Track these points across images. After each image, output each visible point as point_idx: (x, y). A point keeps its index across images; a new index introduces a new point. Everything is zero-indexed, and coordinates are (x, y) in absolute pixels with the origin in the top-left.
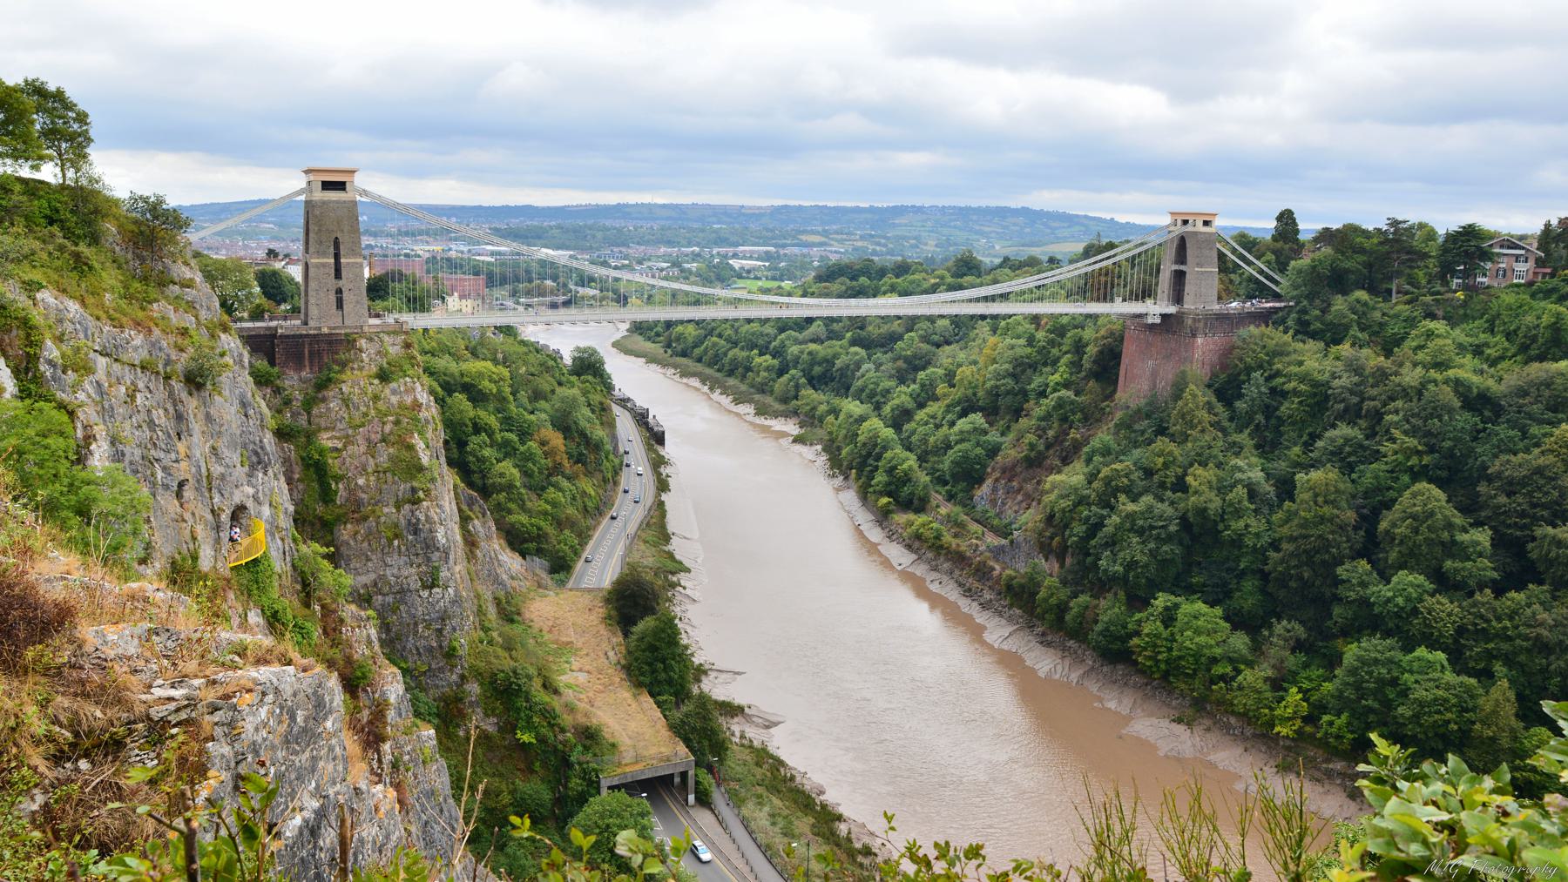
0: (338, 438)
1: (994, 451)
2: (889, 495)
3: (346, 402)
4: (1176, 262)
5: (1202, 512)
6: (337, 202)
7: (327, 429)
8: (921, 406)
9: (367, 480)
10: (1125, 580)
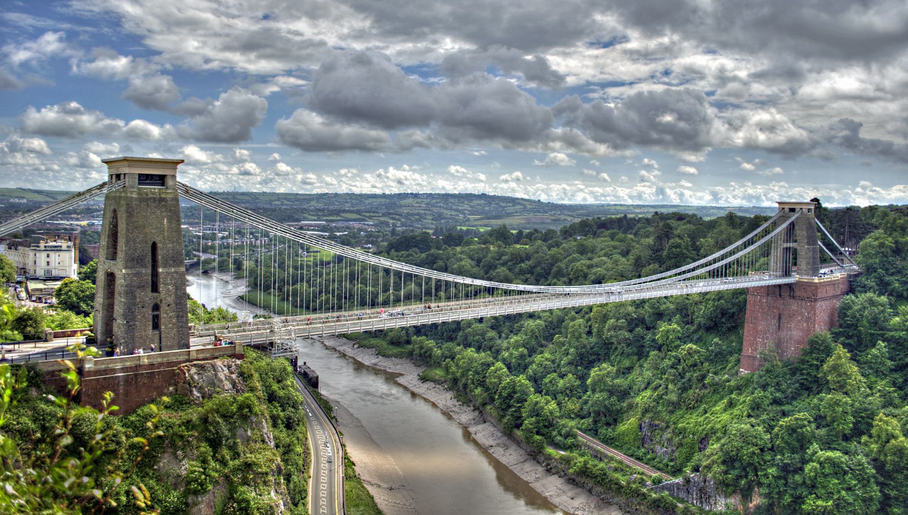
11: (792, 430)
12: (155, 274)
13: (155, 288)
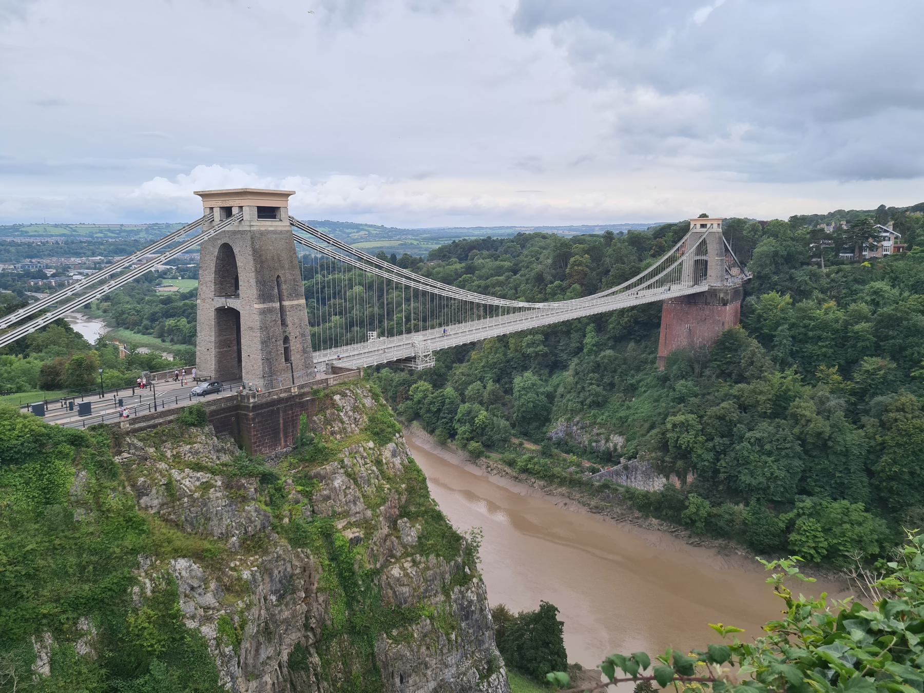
0: (358, 526)
1: (551, 397)
2: (472, 439)
3: (351, 476)
4: (697, 254)
5: (819, 435)
6: (274, 232)
7: (335, 515)
8: (449, 368)
9: (403, 568)
10: (765, 490)
11: (721, 418)
12: (282, 307)
13: (284, 323)
